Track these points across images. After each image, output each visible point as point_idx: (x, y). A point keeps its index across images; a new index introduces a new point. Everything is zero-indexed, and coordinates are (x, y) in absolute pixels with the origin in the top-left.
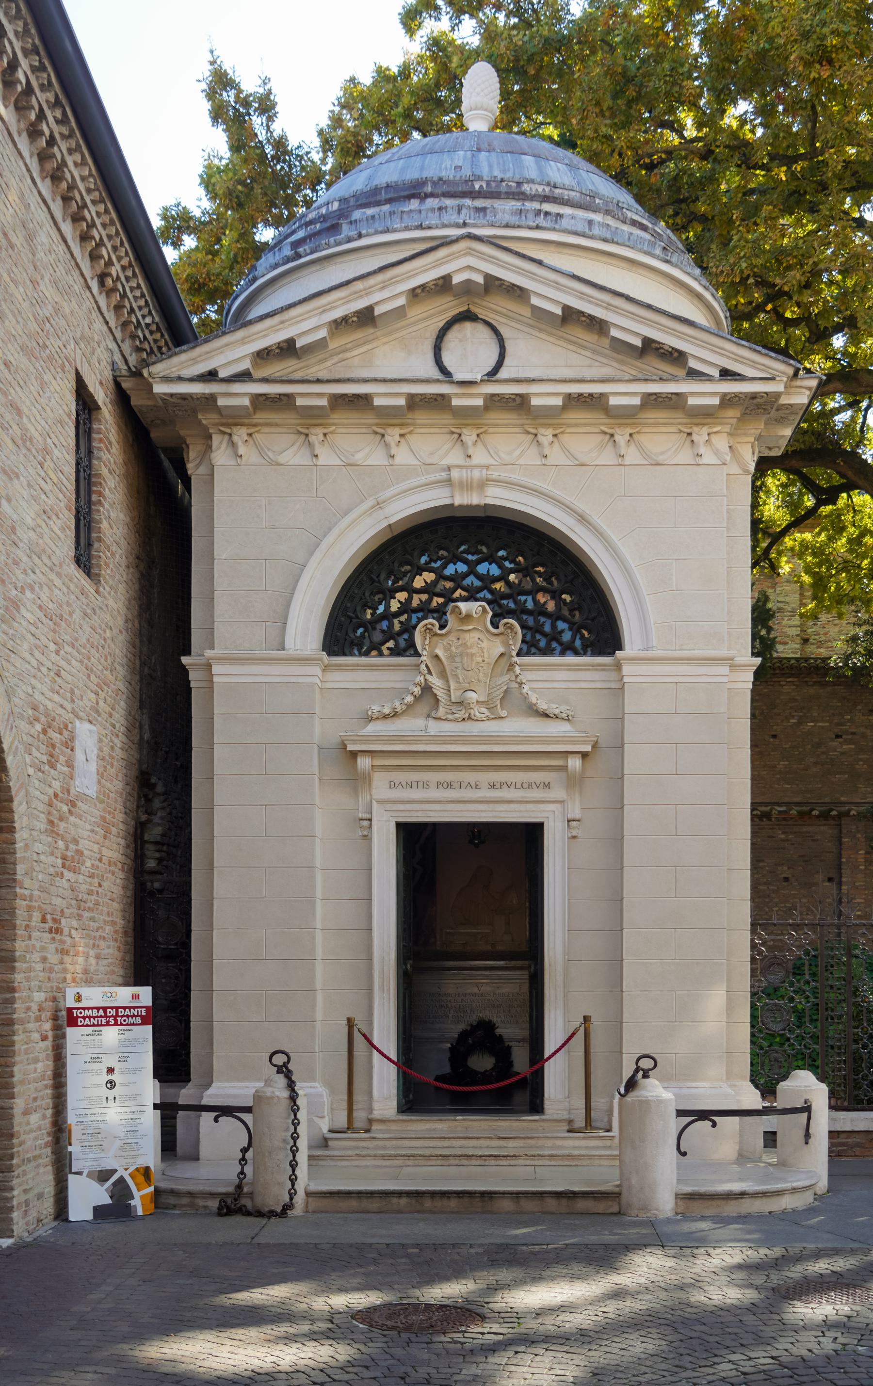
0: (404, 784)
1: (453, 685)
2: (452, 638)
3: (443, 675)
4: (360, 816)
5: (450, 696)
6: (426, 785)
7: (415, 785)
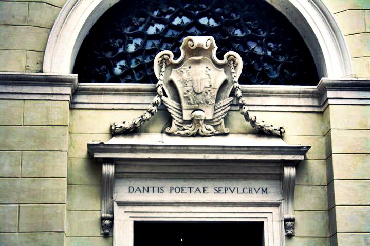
0: (141, 189)
1: (184, 105)
2: (182, 67)
3: (177, 98)
4: (103, 215)
5: (182, 115)
6: (161, 190)
7: (151, 189)
